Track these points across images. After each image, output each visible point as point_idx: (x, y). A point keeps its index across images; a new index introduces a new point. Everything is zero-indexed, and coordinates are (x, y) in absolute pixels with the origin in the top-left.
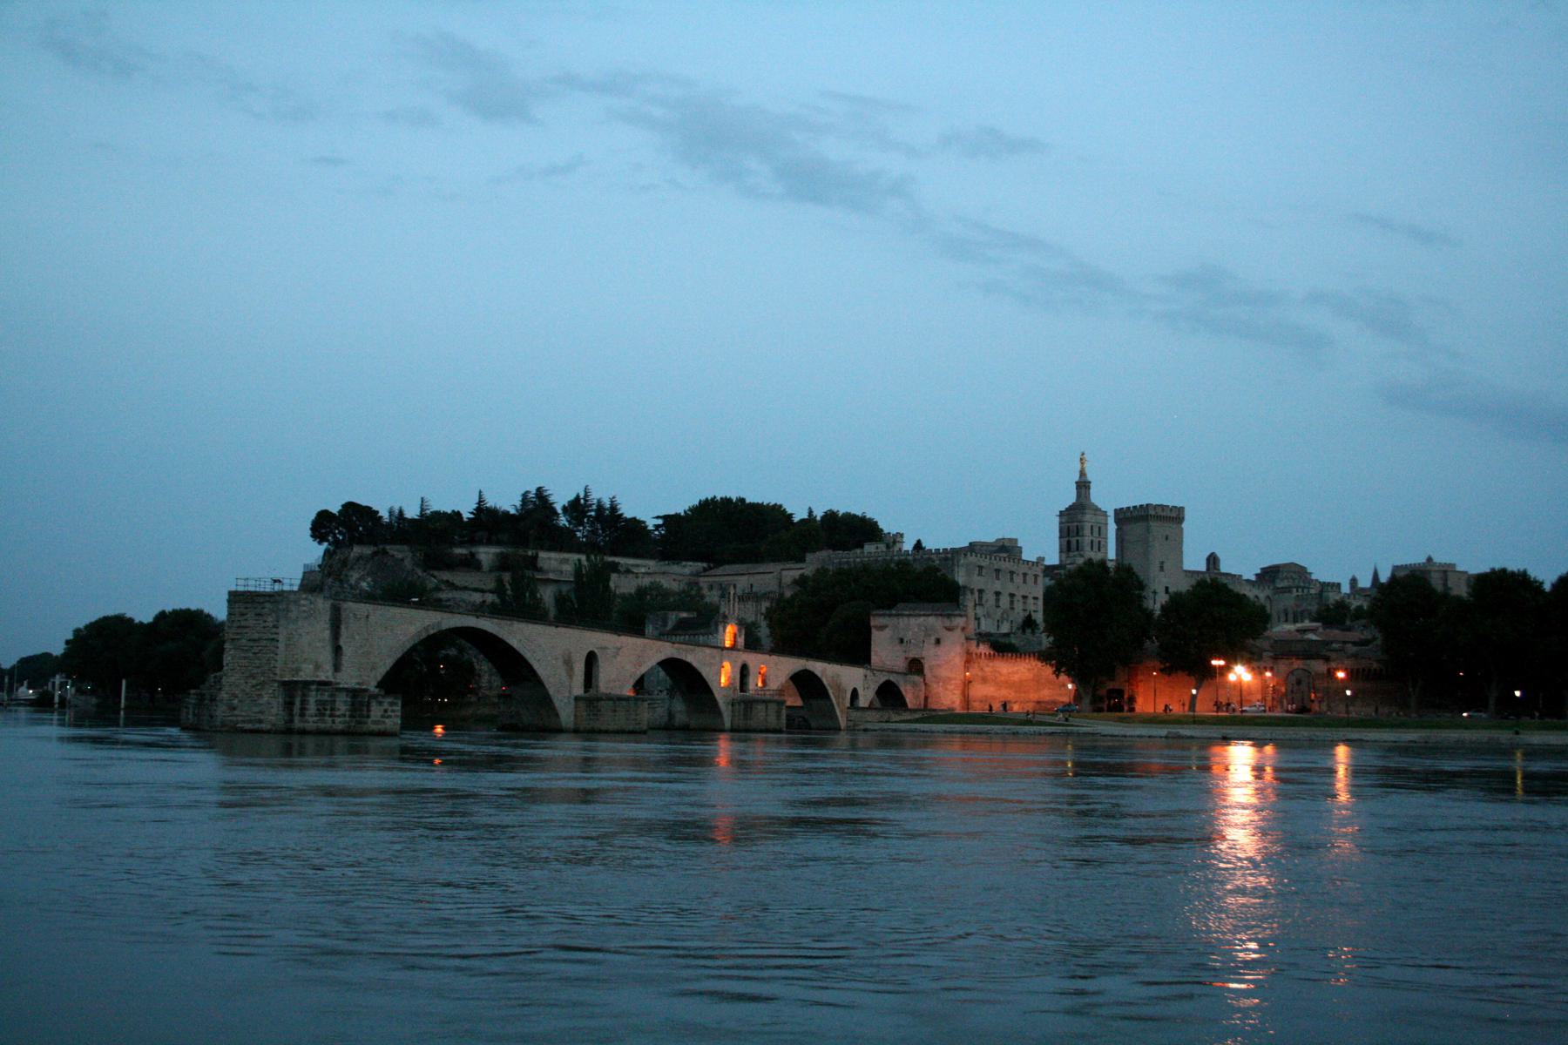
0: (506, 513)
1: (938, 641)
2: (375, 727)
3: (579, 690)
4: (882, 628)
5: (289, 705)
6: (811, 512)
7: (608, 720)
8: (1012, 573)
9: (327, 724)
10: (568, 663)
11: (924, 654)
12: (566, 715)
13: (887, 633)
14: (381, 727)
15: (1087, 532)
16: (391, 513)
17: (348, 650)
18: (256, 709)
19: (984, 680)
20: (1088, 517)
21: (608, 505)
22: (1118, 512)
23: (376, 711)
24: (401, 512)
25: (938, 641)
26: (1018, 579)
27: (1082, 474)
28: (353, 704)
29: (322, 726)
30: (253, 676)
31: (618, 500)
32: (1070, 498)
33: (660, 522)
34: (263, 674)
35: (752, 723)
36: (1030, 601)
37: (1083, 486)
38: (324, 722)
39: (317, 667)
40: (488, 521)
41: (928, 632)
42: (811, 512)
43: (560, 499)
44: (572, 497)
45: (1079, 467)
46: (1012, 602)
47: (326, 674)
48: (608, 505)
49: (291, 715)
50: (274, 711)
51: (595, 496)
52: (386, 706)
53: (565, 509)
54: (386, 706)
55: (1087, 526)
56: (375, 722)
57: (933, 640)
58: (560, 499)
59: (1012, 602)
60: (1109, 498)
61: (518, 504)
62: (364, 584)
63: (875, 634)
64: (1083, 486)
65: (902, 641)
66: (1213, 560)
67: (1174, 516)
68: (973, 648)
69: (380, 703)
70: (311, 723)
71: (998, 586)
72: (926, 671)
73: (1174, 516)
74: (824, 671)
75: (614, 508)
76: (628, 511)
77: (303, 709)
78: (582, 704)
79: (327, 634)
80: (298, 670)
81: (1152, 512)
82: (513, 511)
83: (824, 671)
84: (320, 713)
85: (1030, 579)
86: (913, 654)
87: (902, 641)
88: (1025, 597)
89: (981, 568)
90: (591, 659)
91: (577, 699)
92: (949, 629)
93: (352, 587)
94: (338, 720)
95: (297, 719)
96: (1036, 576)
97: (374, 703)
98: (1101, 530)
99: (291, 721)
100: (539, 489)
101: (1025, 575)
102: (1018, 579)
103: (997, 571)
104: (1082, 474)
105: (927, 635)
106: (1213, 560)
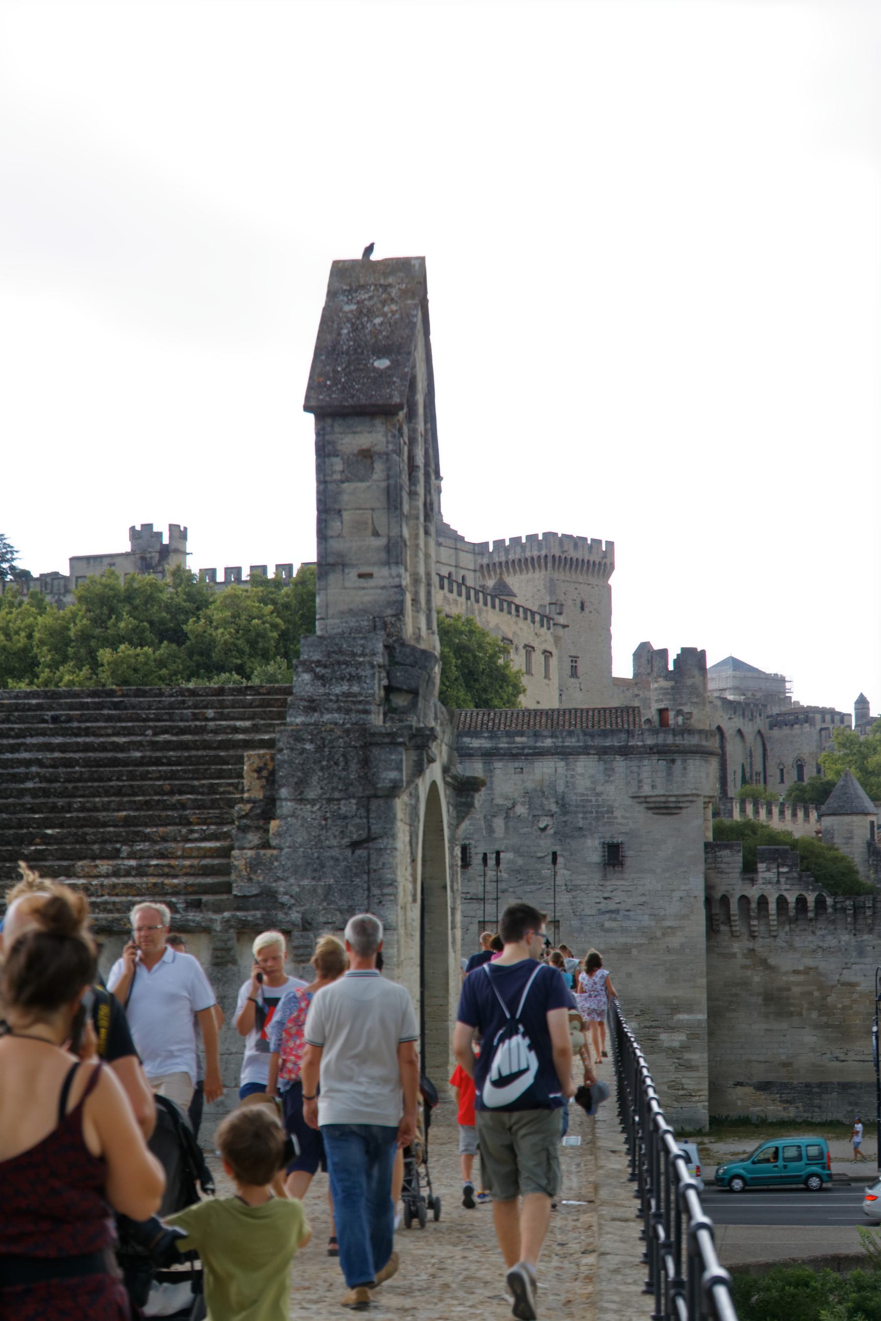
1: (614, 856)
19: (777, 1003)
25: (614, 856)
41: (567, 817)
57: (592, 850)
68: (734, 885)
92: (665, 808)
105: (568, 833)
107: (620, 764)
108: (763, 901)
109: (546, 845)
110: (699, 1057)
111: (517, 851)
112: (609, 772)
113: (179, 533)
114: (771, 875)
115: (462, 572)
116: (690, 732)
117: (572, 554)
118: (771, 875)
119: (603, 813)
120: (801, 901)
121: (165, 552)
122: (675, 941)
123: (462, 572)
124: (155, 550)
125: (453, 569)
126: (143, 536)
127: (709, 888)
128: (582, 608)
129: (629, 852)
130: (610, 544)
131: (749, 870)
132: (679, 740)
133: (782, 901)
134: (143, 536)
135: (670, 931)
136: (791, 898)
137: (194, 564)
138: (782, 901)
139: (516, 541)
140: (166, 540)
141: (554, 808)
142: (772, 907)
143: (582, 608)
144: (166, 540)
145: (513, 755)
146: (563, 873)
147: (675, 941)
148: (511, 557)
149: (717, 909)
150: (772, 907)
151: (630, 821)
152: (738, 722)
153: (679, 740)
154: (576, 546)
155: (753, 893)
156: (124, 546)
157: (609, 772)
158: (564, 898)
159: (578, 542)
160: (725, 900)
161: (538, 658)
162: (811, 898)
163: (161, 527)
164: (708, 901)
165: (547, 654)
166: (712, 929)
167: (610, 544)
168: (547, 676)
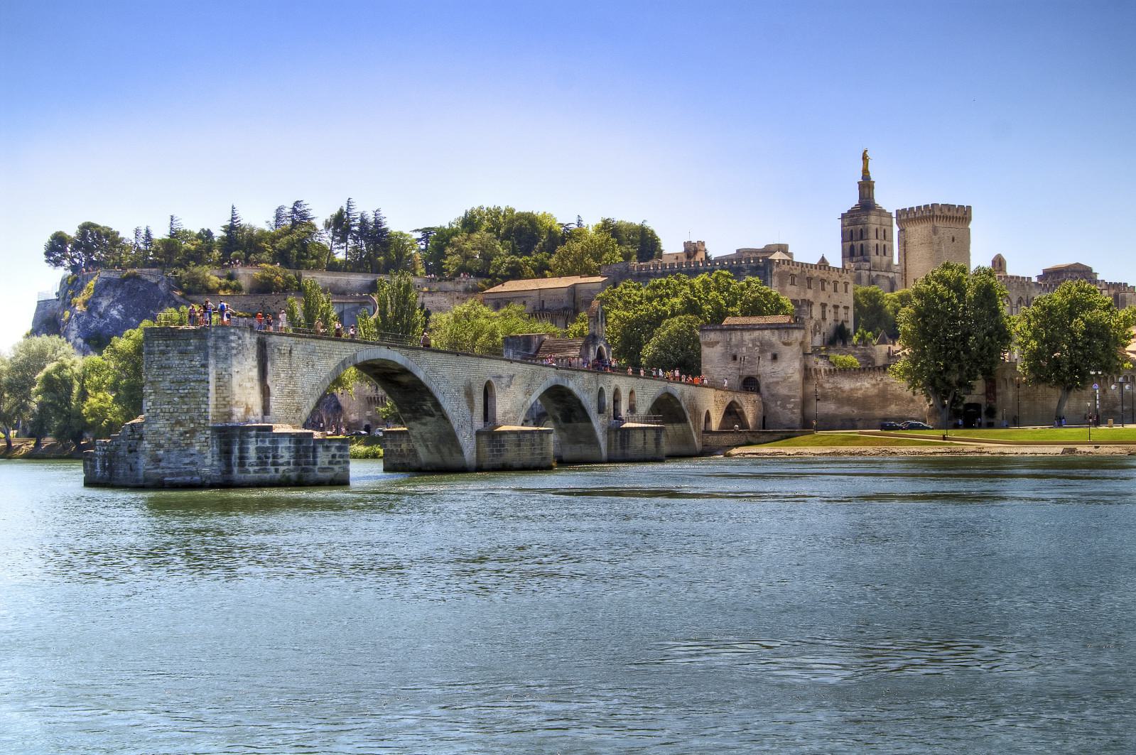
0: (262, 231)
1: (775, 357)
2: (321, 475)
3: (479, 424)
4: (712, 344)
5: (226, 453)
6: (579, 224)
7: (510, 455)
8: (823, 281)
9: (271, 473)
10: (469, 394)
11: (761, 370)
12: (468, 447)
13: (719, 349)
14: (329, 475)
15: (872, 234)
16: (137, 232)
17: (274, 391)
18: (187, 460)
20: (873, 218)
21: (371, 219)
22: (900, 213)
23: (323, 458)
24: (148, 234)
25: (775, 357)
26: (829, 288)
27: (865, 172)
28: (297, 451)
29: (267, 476)
30: (179, 423)
31: (383, 214)
32: (853, 200)
33: (419, 235)
34: (192, 420)
35: (630, 452)
36: (841, 311)
37: (866, 186)
38: (265, 470)
39: (248, 410)
40: (239, 243)
41: (764, 346)
42: (579, 224)
43: (320, 214)
44: (335, 211)
46: (824, 313)
47: (256, 417)
48: (371, 219)
49: (229, 465)
50: (208, 461)
51: (357, 211)
52: (333, 451)
53: (328, 225)
54: (333, 451)
55: (873, 228)
56: (323, 470)
57: (769, 356)
58: (320, 214)
59: (824, 313)
61: (272, 220)
62: (114, 313)
63: (706, 351)
64: (866, 186)
65: (735, 358)
66: (999, 262)
69: (327, 448)
70: (252, 473)
71: (823, 298)
72: (763, 388)
74: (682, 393)
75: (378, 223)
76: (394, 225)
77: (242, 458)
78: (484, 438)
79: (255, 373)
80: (230, 414)
81: (938, 213)
82: (267, 229)
83: (682, 393)
84: (262, 462)
85: (841, 287)
86: (746, 373)
87: (735, 358)
88: (836, 307)
89: (793, 276)
90: (488, 391)
91: (478, 433)
93: (101, 316)
94: (282, 468)
95: (236, 469)
96: (846, 284)
97: (320, 450)
98: (886, 236)
99: (230, 472)
100: (297, 203)
101: (836, 283)
102: (829, 288)
103: (810, 279)
104: (865, 172)
105: (762, 351)
106: (999, 262)
107: (776, 332)
109: (757, 355)
110: (797, 411)
111: (749, 356)
112: (773, 334)
114: (822, 362)
115: (884, 227)
117: (950, 214)
119: (771, 345)
123: (884, 227)
125: (878, 226)
128: (953, 240)
129: (779, 356)
130: (969, 207)
133: (825, 371)
135: (790, 377)
136: (827, 368)
139: (919, 208)
142: (823, 371)
143: (953, 240)
145: (748, 330)
146: (761, 362)
148: (917, 216)
150: (823, 371)
154: (949, 210)
156: (681, 249)
157: (773, 334)
159: (949, 207)
160: (810, 369)
162: (832, 368)
167: (969, 207)
168: (846, 291)
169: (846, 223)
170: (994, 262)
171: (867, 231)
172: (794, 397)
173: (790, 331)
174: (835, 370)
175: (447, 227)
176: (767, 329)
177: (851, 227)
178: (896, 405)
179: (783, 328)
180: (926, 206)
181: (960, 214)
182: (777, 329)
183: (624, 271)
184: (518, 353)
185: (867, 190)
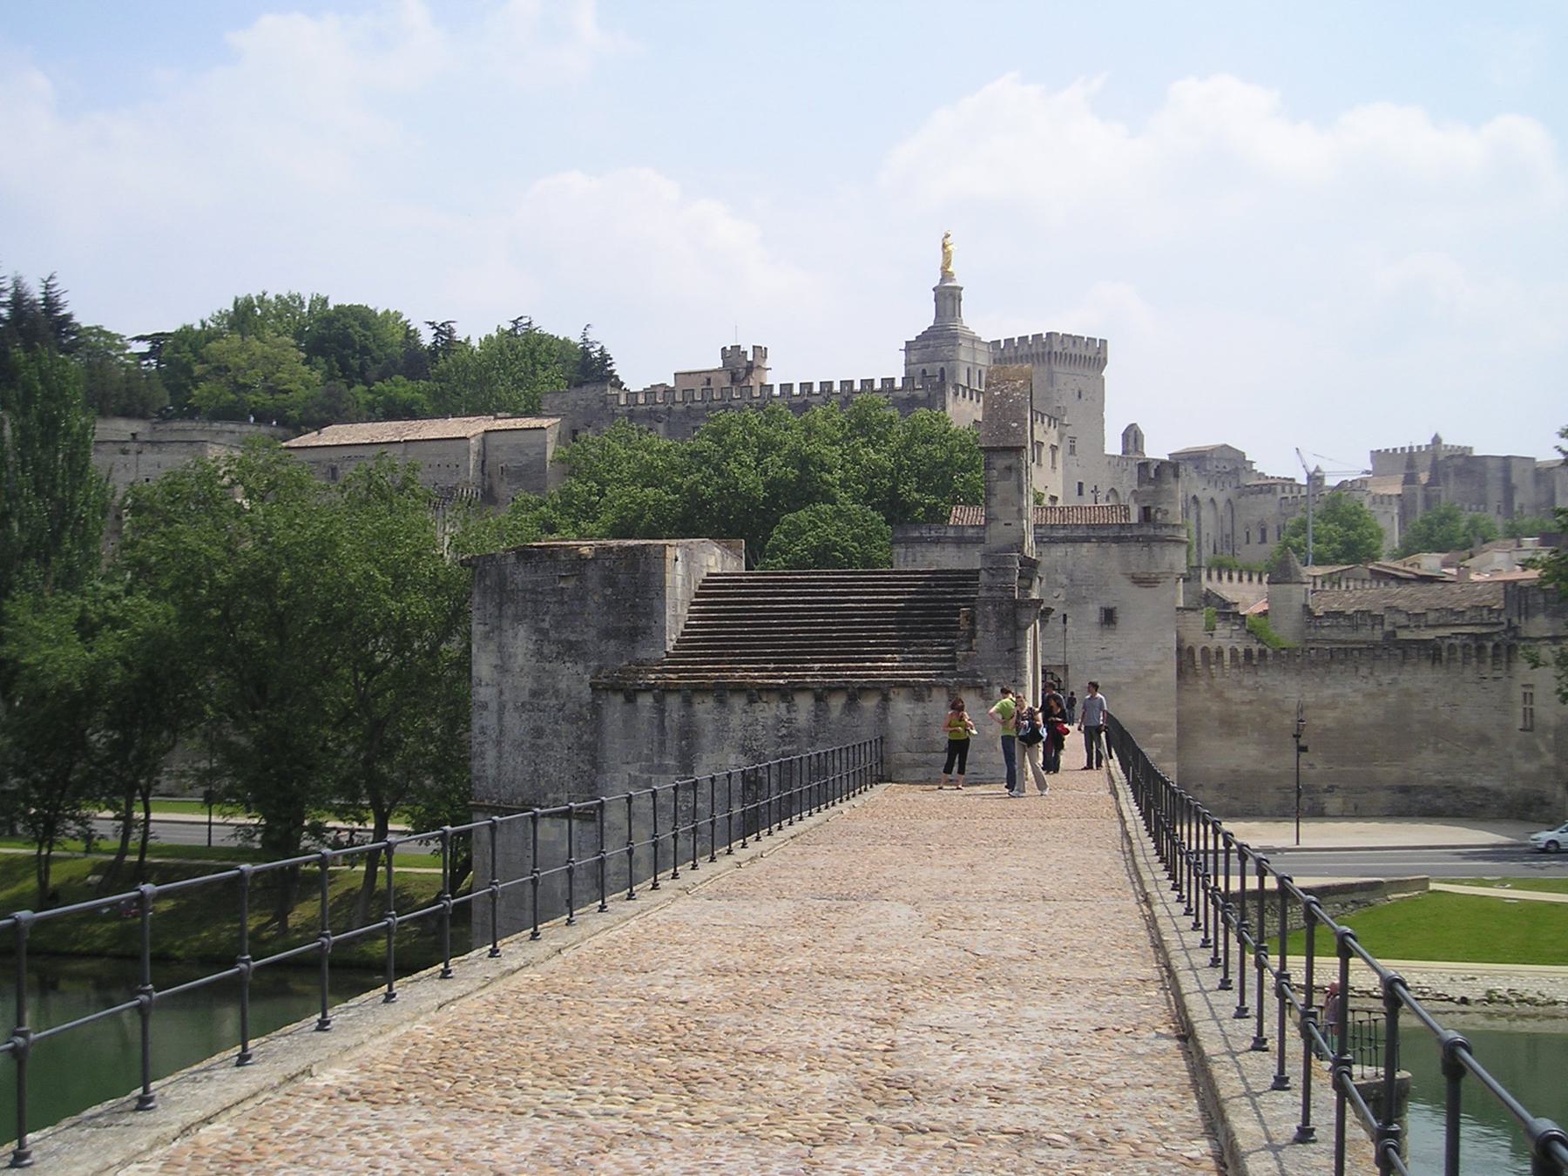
1: (1109, 617)
19: (1229, 725)
25: (1109, 617)
27: (946, 275)
31: (60, 285)
32: (924, 318)
33: (145, 347)
37: (947, 298)
45: (939, 262)
48: (37, 294)
57: (1093, 613)
60: (990, 320)
64: (947, 298)
66: (1132, 436)
67: (1086, 357)
73: (1086, 357)
75: (51, 303)
81: (1057, 348)
104: (946, 275)
106: (1132, 436)
108: (1220, 653)
113: (760, 352)
114: (1226, 632)
116: (1166, 526)
117: (1075, 351)
118: (1226, 632)
120: (1248, 653)
121: (750, 368)
122: (1154, 680)
124: (740, 366)
126: (732, 355)
127: (1180, 641)
129: (1120, 615)
131: (1210, 628)
132: (1158, 532)
133: (1234, 652)
134: (732, 355)
136: (1241, 650)
137: (775, 375)
138: (1234, 652)
140: (750, 358)
141: (1066, 582)
142: (1227, 655)
144: (750, 358)
147: (1154, 680)
148: (1020, 352)
149: (1185, 655)
150: (1227, 655)
151: (1124, 594)
152: (1212, 492)
153: (1158, 532)
155: (1212, 645)
156: (718, 363)
158: (1071, 649)
159: (1075, 340)
160: (1191, 650)
161: (1046, 451)
162: (1255, 648)
163: (747, 348)
164: (1179, 650)
165: (1054, 448)
166: (1181, 673)
168: (1054, 468)
169: (914, 359)
170: (1125, 435)
171: (954, 373)
172: (1164, 728)
173: (1156, 548)
174: (1262, 653)
175: (198, 327)
176: (1087, 540)
177: (924, 366)
178: (1438, 751)
179: (1136, 539)
180: (1037, 337)
181: (1090, 353)
182: (1118, 540)
183: (597, 406)
184: (572, 650)
185: (949, 303)
